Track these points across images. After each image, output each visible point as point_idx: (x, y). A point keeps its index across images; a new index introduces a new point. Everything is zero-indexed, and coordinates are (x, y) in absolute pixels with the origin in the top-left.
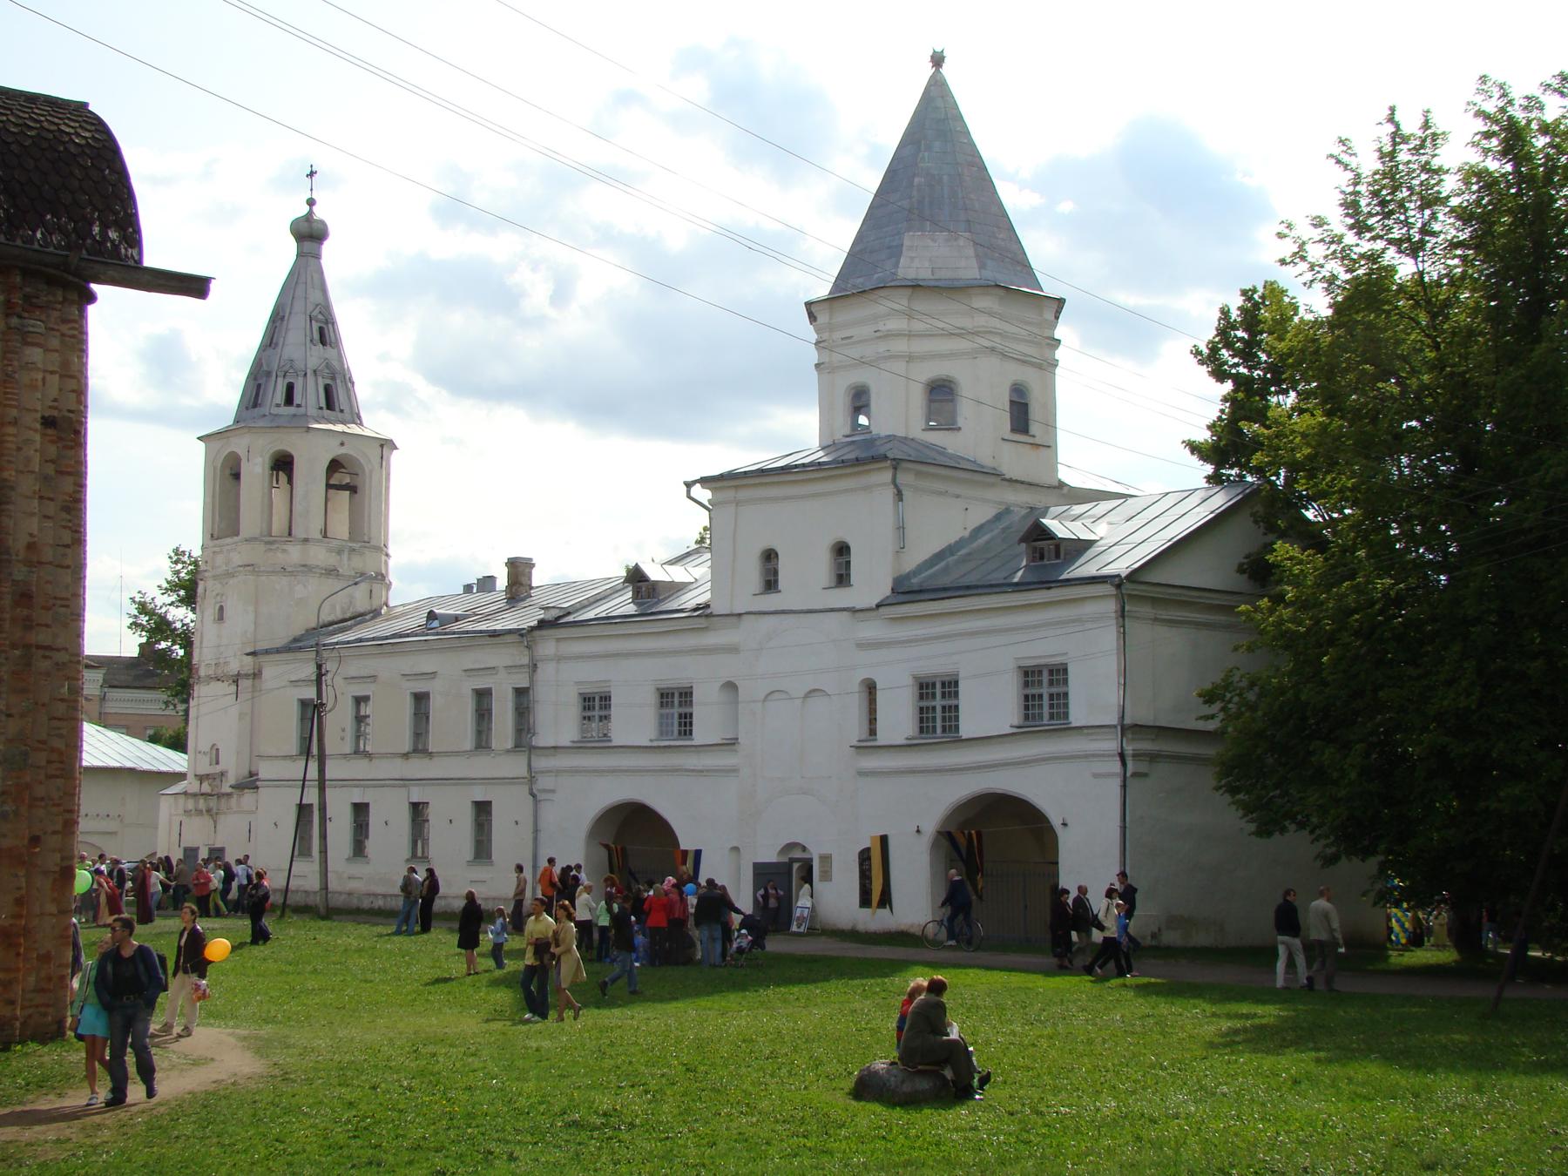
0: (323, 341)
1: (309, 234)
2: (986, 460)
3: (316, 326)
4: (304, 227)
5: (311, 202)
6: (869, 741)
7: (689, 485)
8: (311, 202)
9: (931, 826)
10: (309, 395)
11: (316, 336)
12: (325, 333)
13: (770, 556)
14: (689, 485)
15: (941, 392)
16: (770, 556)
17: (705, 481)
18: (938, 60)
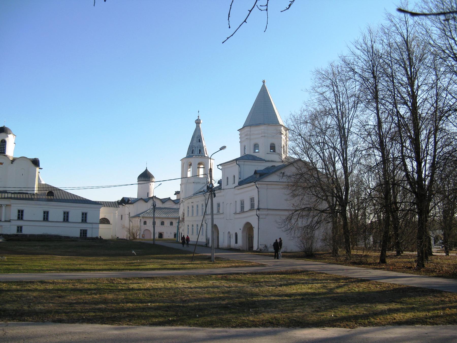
0: (199, 141)
1: (198, 122)
2: (263, 158)
3: (198, 139)
4: (197, 122)
5: (198, 117)
6: (236, 213)
7: (218, 166)
8: (198, 117)
9: (242, 228)
10: (197, 152)
11: (198, 141)
12: (200, 141)
13: (228, 178)
14: (218, 166)
15: (256, 146)
16: (228, 178)
17: (220, 165)
18: (264, 82)
